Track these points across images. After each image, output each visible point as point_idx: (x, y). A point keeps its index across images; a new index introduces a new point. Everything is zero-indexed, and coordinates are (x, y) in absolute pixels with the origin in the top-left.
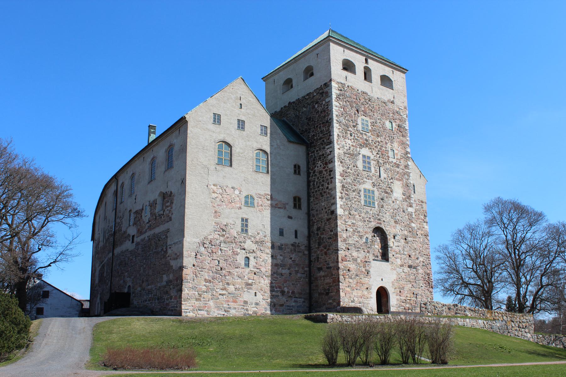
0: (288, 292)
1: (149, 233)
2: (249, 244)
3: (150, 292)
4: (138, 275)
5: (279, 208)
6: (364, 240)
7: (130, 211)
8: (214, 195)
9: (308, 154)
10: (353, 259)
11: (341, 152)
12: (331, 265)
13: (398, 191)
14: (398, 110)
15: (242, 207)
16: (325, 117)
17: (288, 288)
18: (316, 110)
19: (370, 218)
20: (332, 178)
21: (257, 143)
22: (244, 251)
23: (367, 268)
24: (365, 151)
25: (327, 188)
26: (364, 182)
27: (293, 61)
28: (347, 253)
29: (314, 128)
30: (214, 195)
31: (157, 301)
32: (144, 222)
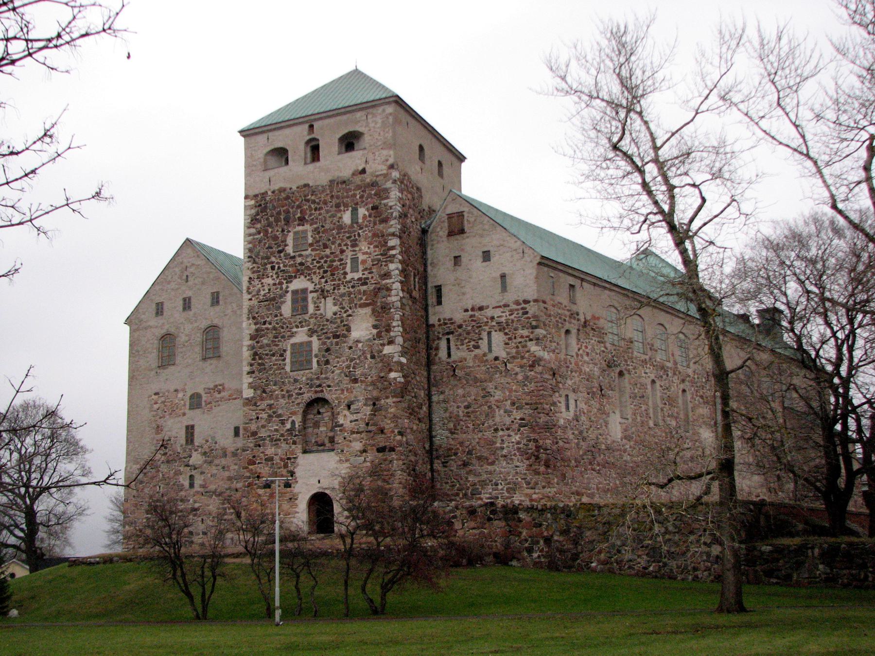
2: (196, 458)
6: (288, 426)
8: (156, 406)
10: (266, 460)
11: (255, 302)
13: (362, 328)
15: (187, 411)
19: (301, 389)
23: (291, 468)
24: (298, 284)
26: (292, 335)
30: (156, 406)
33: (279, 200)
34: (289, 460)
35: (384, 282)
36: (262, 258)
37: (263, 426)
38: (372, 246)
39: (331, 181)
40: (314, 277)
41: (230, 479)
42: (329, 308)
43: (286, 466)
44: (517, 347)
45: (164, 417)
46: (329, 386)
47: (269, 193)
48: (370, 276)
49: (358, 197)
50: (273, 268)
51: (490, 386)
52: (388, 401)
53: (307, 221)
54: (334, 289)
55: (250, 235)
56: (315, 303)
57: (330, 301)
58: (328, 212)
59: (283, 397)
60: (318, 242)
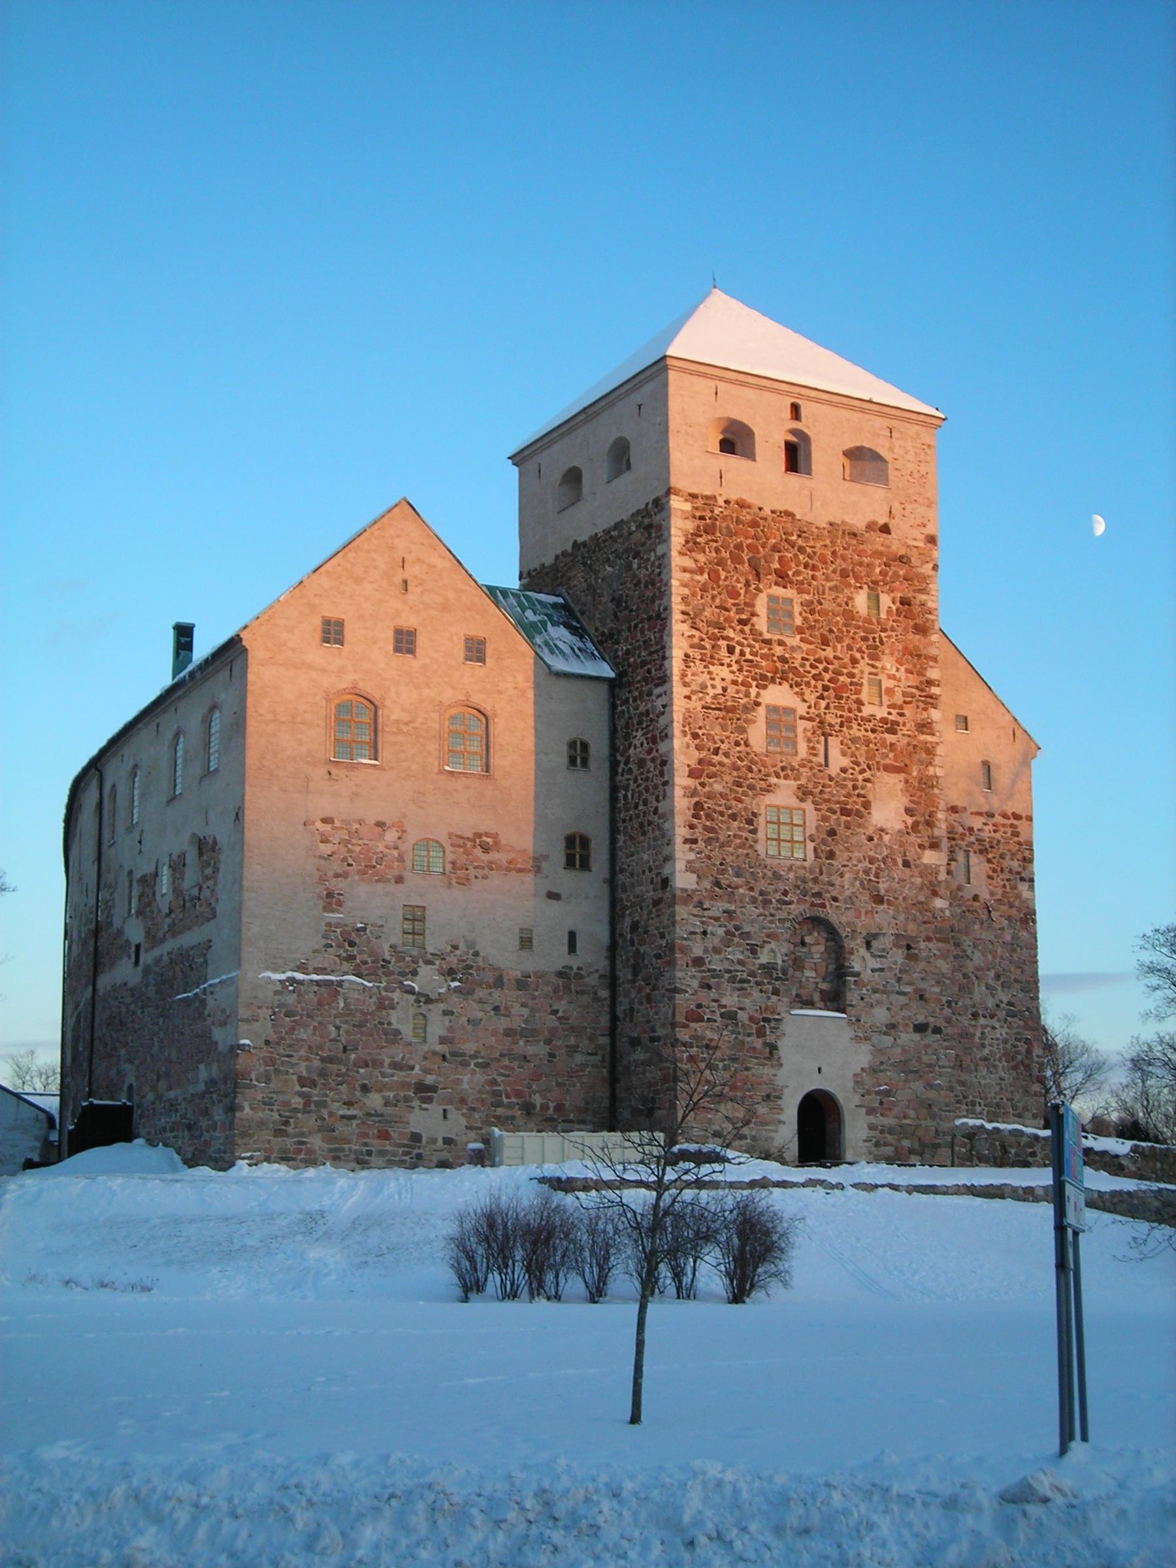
0: (545, 1107)
1: (170, 945)
3: (172, 1107)
4: (148, 1060)
5: (520, 871)
7: (130, 873)
9: (613, 707)
10: (722, 1015)
11: (696, 704)
12: (660, 1032)
14: (902, 552)
16: (653, 601)
17: (544, 1097)
18: (634, 576)
19: (785, 893)
20: (666, 783)
21: (454, 688)
22: (412, 998)
23: (770, 1038)
24: (778, 695)
25: (656, 811)
26: (769, 789)
27: (583, 416)
28: (704, 997)
29: (629, 628)
31: (186, 1133)
32: (159, 910)
33: (738, 521)
34: (766, 1023)
35: (922, 737)
36: (709, 624)
37: (717, 951)
38: (902, 669)
39: (831, 524)
40: (807, 691)
41: (509, 1033)
42: (838, 761)
43: (761, 1033)
44: (1004, 886)
45: (345, 875)
46: (835, 899)
47: (721, 502)
48: (900, 720)
49: (878, 570)
50: (731, 650)
51: (967, 942)
52: (931, 945)
53: (791, 582)
54: (841, 726)
55: (685, 570)
56: (809, 741)
57: (834, 743)
58: (828, 579)
59: (754, 900)
60: (811, 628)
